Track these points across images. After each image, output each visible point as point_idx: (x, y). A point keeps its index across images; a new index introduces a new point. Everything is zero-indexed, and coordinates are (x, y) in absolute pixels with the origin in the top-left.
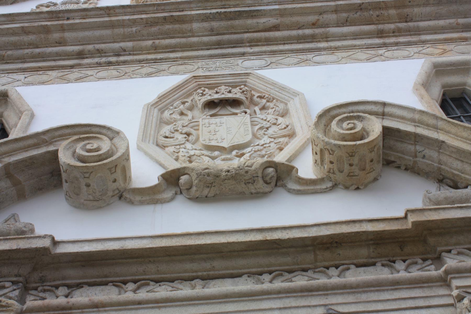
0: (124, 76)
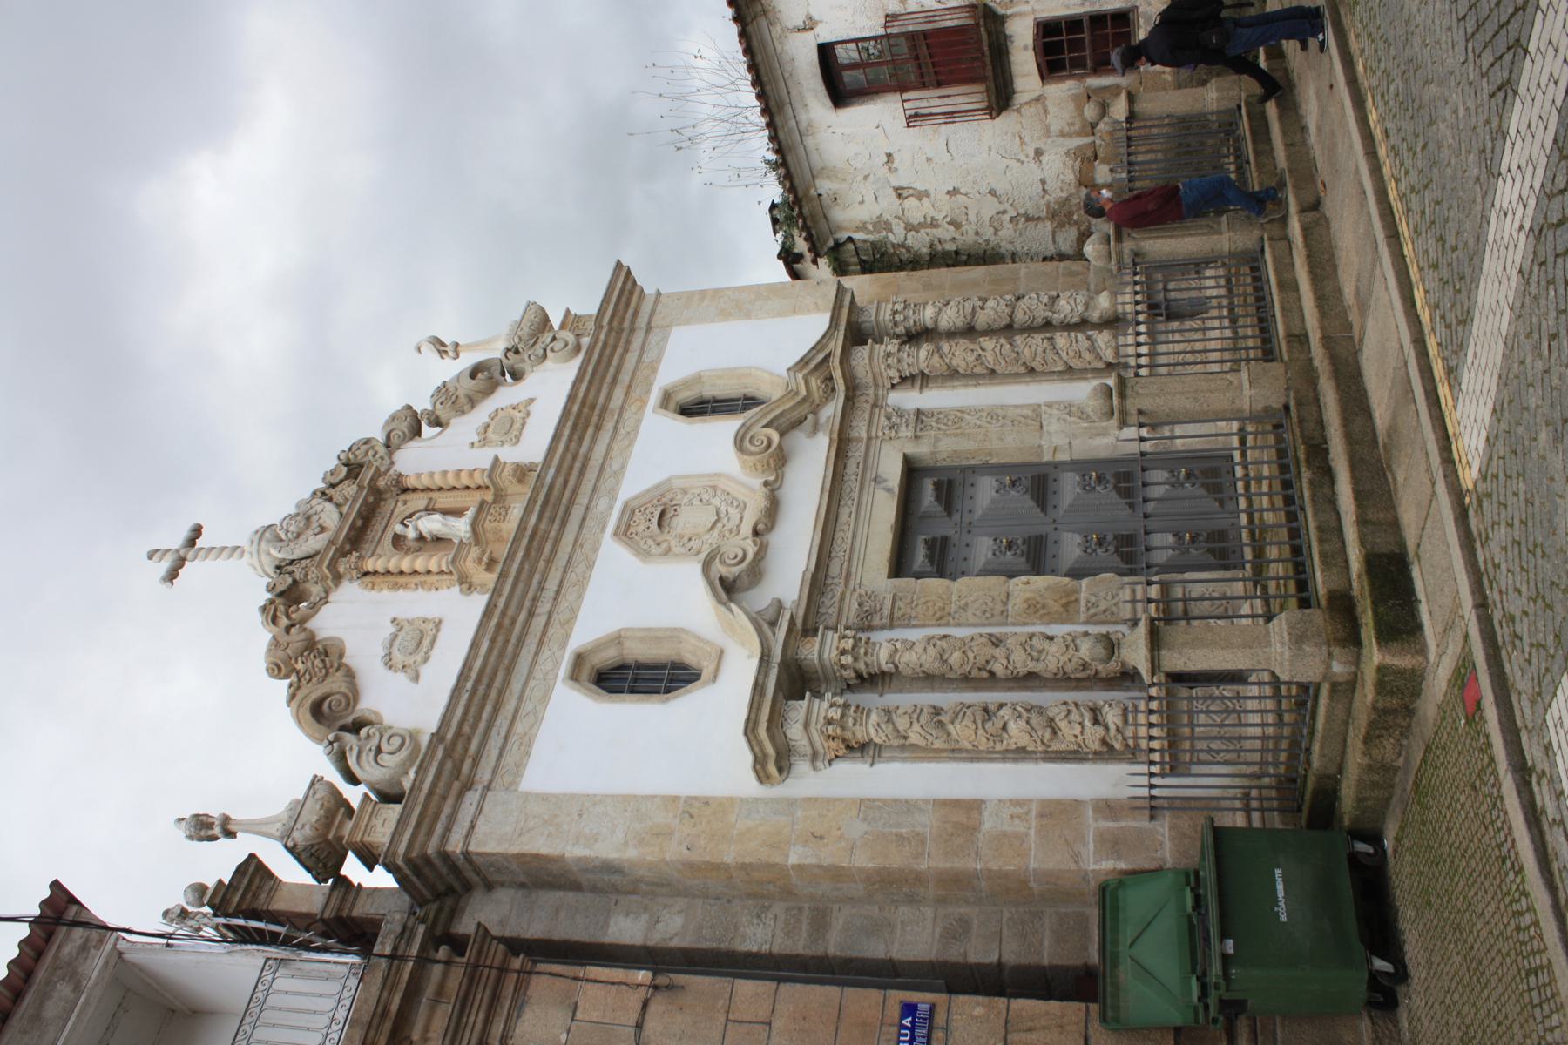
0: (582, 584)
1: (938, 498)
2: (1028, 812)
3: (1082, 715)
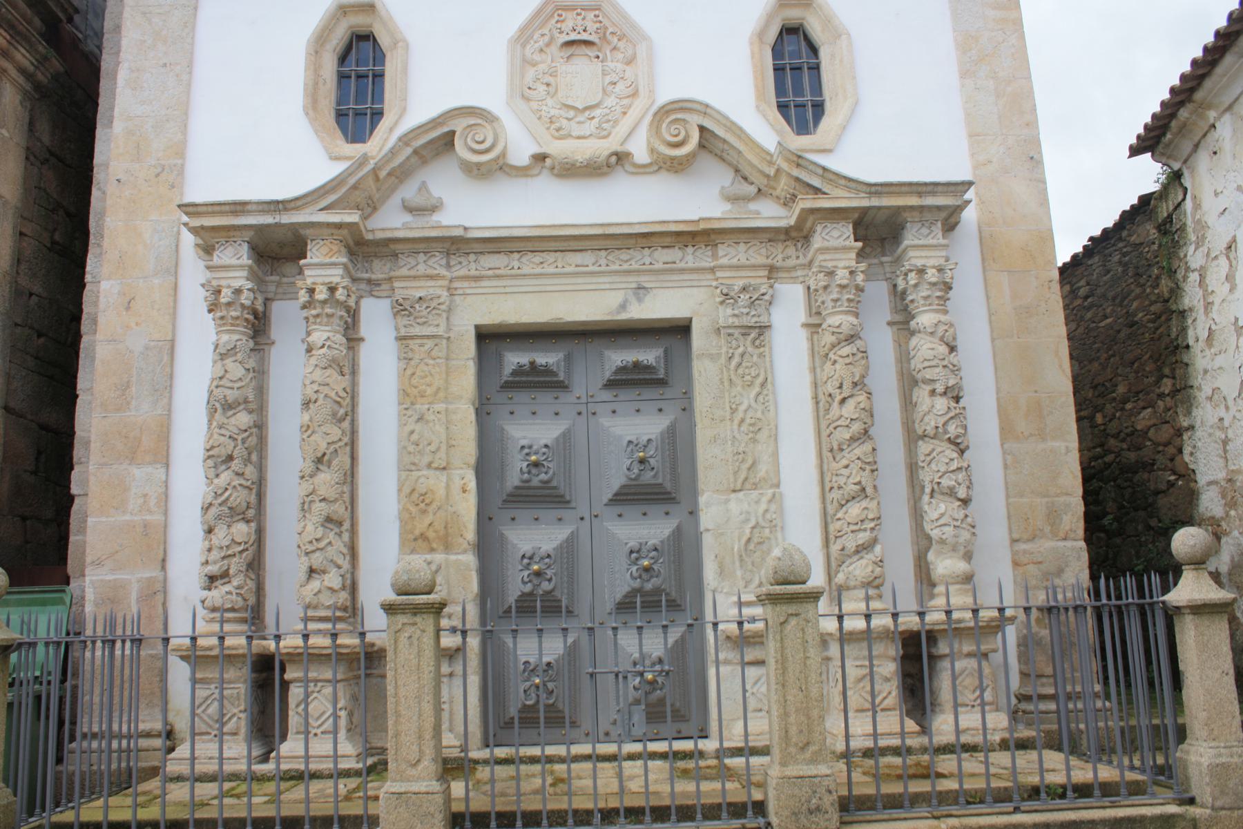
1: (622, 369)
2: (150, 512)
3: (215, 563)
